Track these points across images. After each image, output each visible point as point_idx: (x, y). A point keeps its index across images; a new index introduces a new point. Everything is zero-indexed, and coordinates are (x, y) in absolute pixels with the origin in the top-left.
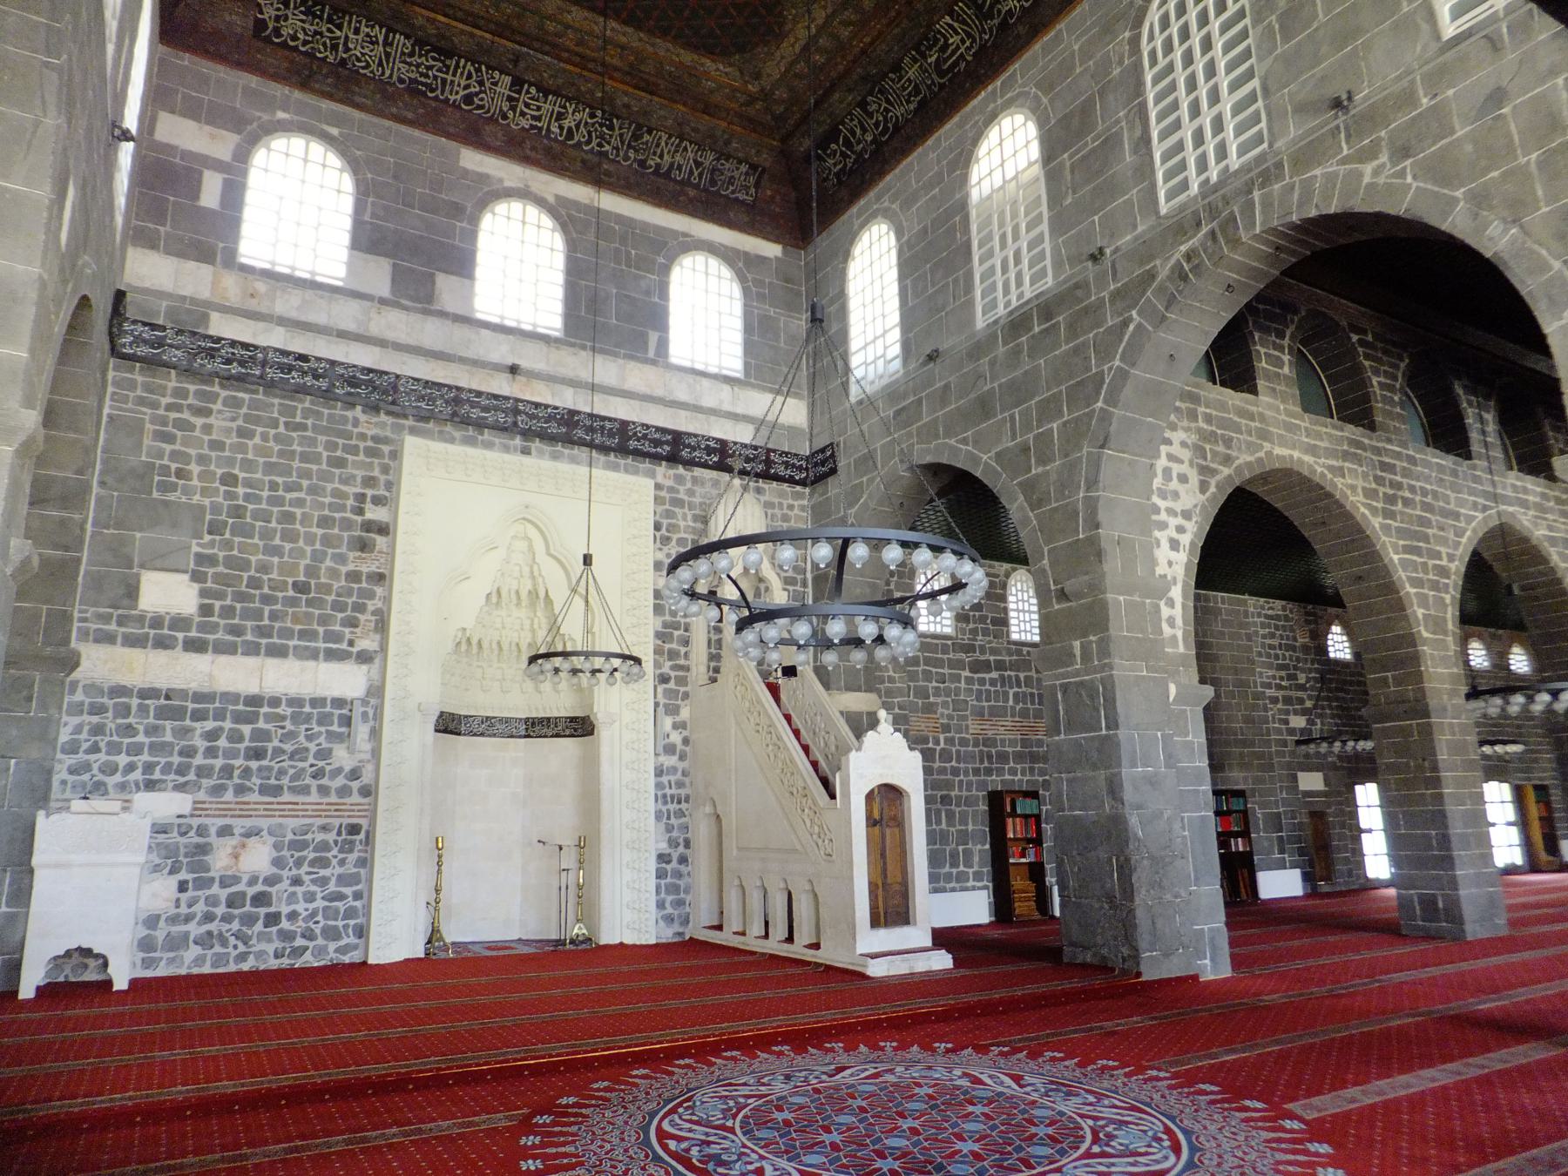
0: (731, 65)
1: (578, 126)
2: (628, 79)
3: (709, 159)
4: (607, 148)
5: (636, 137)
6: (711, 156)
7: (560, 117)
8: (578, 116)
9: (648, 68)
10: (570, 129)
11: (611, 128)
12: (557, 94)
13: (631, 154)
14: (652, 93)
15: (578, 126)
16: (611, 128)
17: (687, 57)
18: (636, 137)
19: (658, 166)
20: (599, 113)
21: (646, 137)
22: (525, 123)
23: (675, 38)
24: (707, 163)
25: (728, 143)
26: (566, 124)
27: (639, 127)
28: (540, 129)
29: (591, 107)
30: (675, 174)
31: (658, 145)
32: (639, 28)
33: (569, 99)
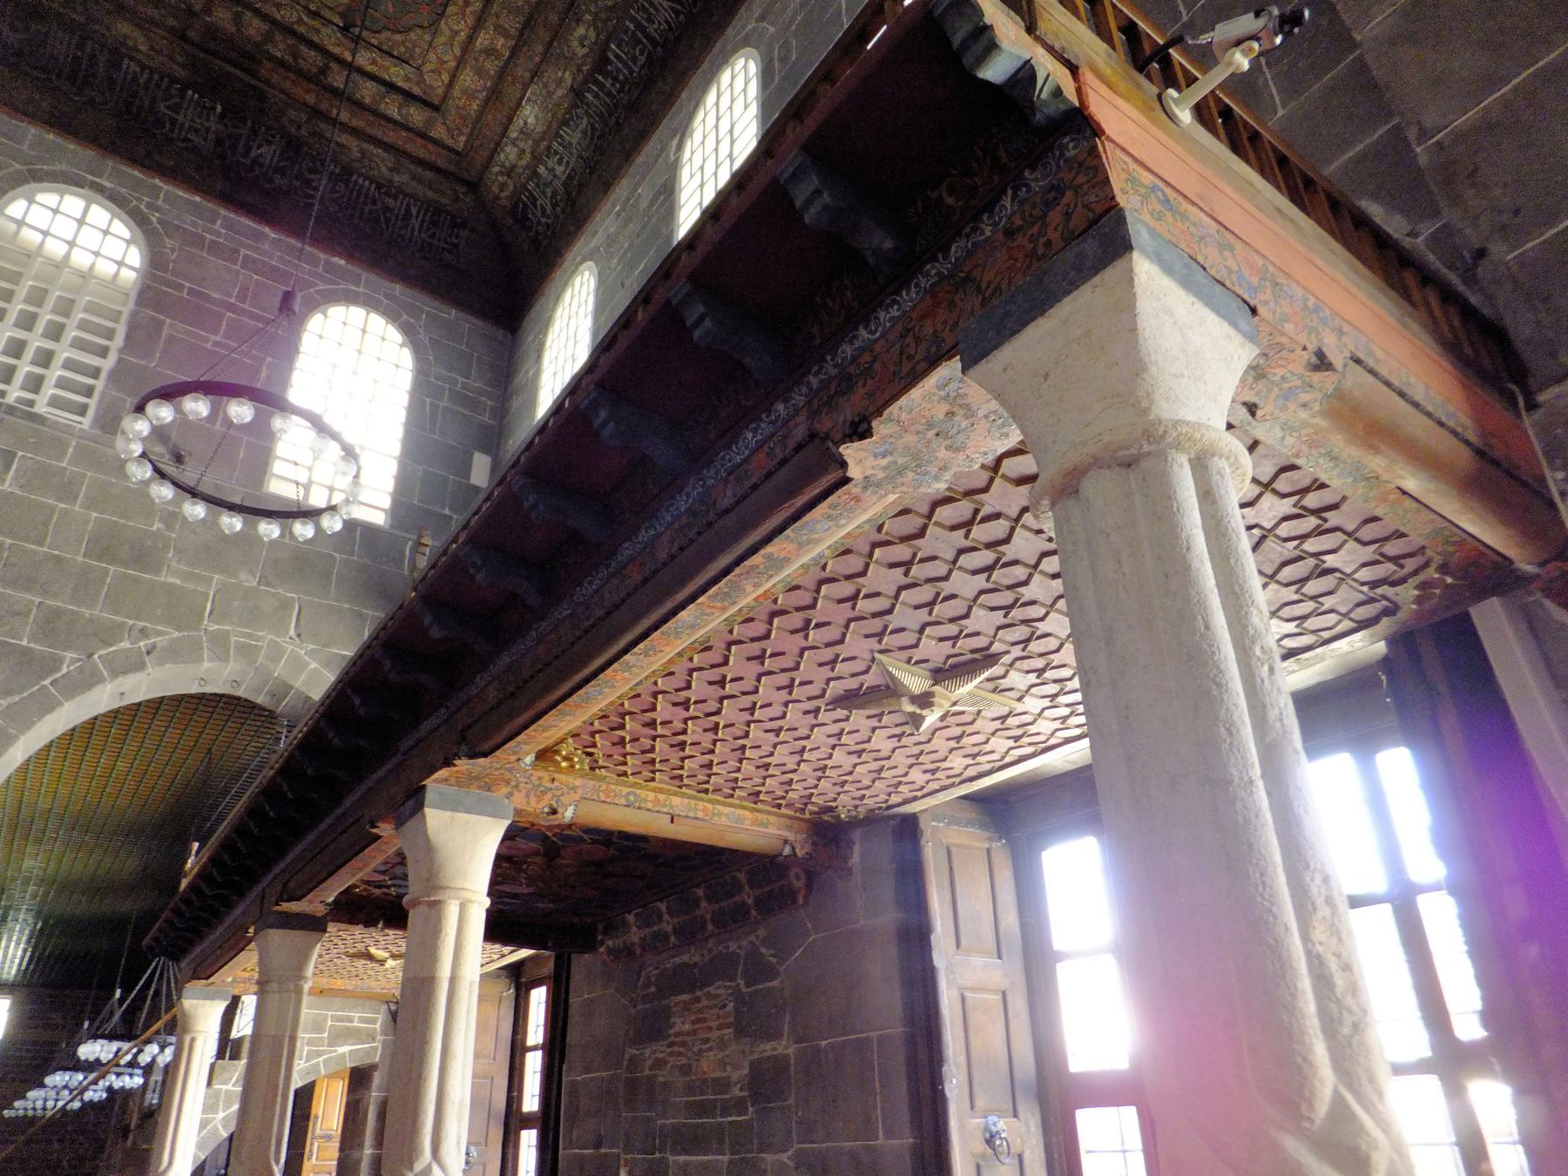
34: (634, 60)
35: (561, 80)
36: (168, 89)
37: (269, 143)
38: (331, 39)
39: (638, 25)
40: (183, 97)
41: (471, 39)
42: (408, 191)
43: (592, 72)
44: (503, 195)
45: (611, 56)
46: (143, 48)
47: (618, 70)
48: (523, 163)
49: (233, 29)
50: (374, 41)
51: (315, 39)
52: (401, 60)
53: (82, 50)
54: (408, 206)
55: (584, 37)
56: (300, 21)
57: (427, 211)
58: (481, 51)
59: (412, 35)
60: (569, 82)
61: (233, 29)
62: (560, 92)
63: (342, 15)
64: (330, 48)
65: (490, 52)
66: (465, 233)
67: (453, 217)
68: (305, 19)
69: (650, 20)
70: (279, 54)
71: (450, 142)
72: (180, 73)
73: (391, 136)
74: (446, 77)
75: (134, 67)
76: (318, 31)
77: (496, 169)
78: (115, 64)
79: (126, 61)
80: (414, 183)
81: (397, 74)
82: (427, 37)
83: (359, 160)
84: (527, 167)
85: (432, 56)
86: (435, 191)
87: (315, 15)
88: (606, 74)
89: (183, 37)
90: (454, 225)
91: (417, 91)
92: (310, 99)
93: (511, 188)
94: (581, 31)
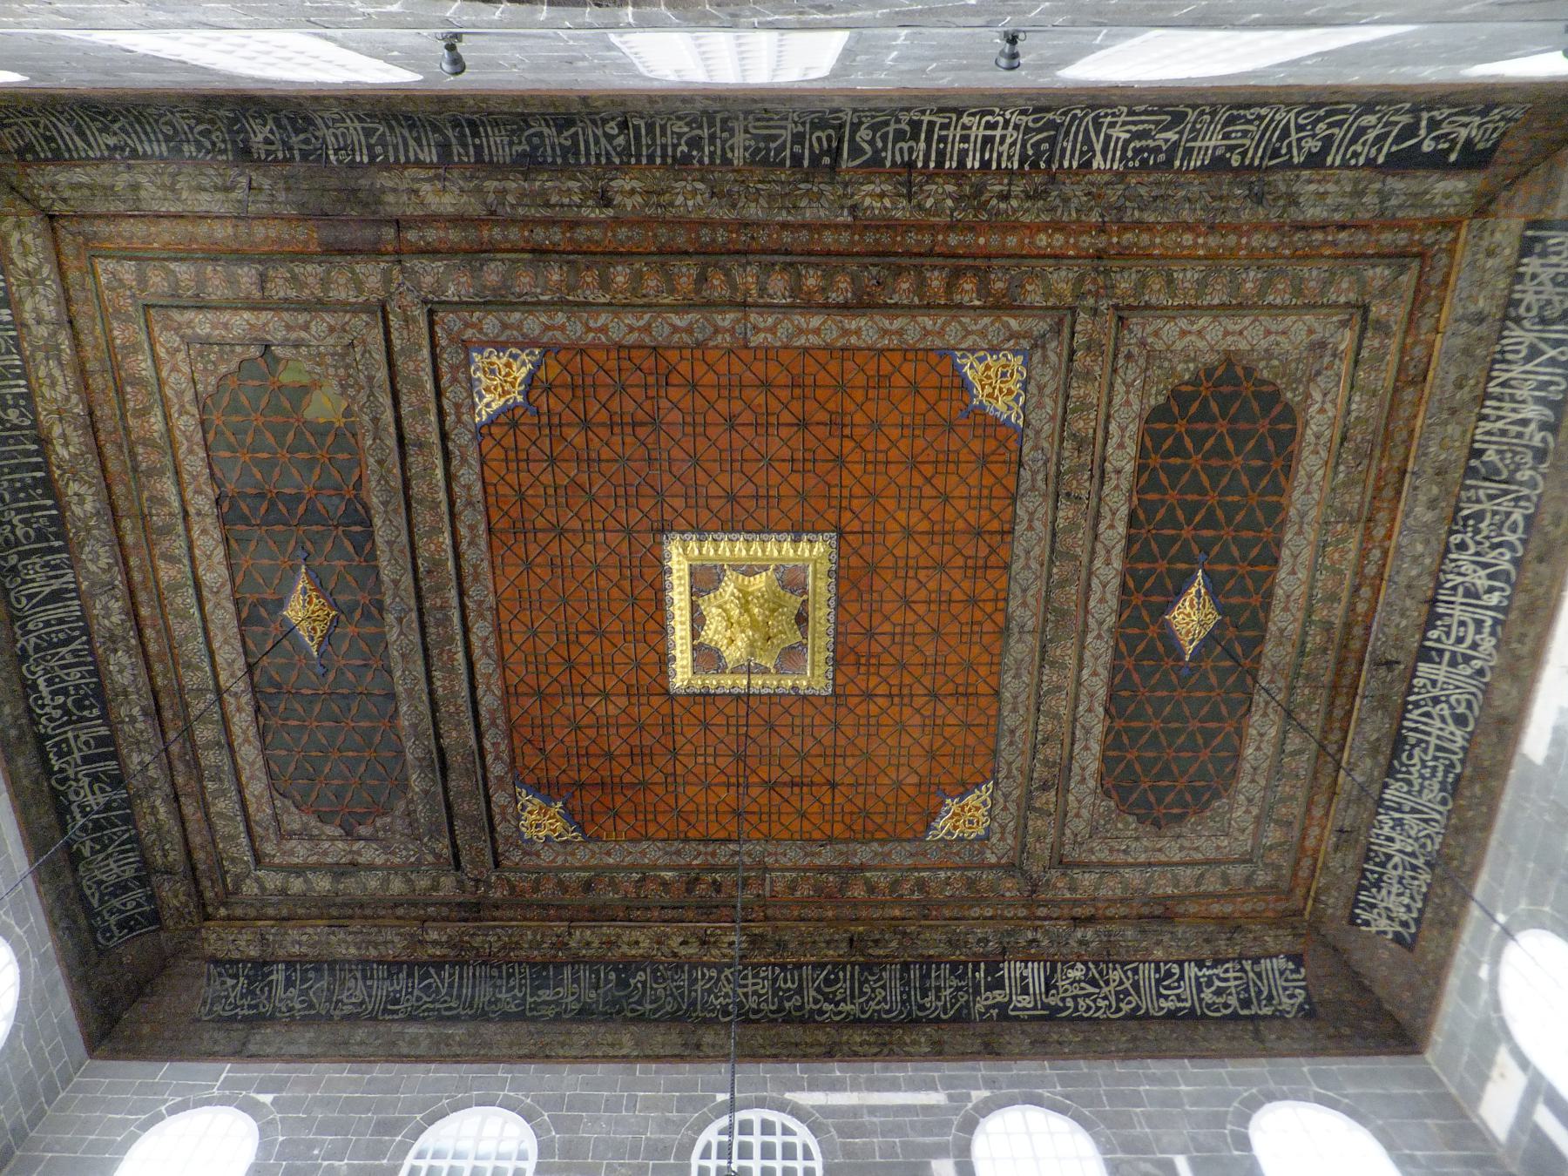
0: (1308, 396)
1: (1485, 566)
2: (1382, 516)
3: (1521, 337)
4: (1517, 516)
5: (1491, 474)
6: (1515, 333)
7: (1471, 593)
8: (1467, 568)
9: (1353, 500)
10: (1490, 577)
11: (1479, 516)
12: (1434, 602)
13: (1525, 475)
14: (1405, 472)
15: (1485, 566)
16: (1479, 516)
17: (1311, 462)
18: (1491, 474)
19: (1544, 426)
20: (1456, 539)
21: (1491, 456)
22: (1488, 643)
23: (1280, 492)
24: (1530, 337)
25: (1480, 319)
26: (1482, 582)
27: (1471, 472)
28: (1496, 621)
29: (1447, 550)
30: (1554, 393)
31: (1503, 433)
32: (1279, 543)
33: (1439, 585)
34: (25, 522)
35: (66, 445)
36: (386, 152)
37: (268, 141)
38: (274, 325)
39: (52, 551)
40: (370, 148)
41: (167, 417)
42: (105, 167)
43: (49, 472)
44: (16, 236)
45: (49, 502)
46: (426, 187)
47: (29, 498)
48: (28, 306)
49: (358, 268)
50: (238, 349)
51: (285, 315)
52: (206, 342)
53: (474, 145)
54: (89, 145)
55: (82, 502)
56: (306, 327)
57: (69, 150)
58: (151, 406)
59: (213, 380)
60: (59, 449)
61: (358, 268)
62: (57, 431)
63: (277, 360)
64: (270, 314)
65: (143, 413)
66: (11, 145)
67: (37, 159)
68: (303, 334)
69: (46, 565)
70: (309, 268)
71: (111, 265)
72: (385, 180)
73: (165, 233)
74: (162, 352)
75: (425, 157)
76: (288, 328)
77: (45, 271)
78: (444, 148)
79: (435, 159)
80: (107, 181)
81: (202, 323)
82: (200, 387)
83: (174, 176)
84: (21, 301)
85: (186, 369)
86: (80, 186)
87: (297, 345)
88: (37, 482)
89: (398, 224)
90: (29, 147)
91: (176, 315)
92: (260, 231)
93: (15, 256)
94: (88, 507)
